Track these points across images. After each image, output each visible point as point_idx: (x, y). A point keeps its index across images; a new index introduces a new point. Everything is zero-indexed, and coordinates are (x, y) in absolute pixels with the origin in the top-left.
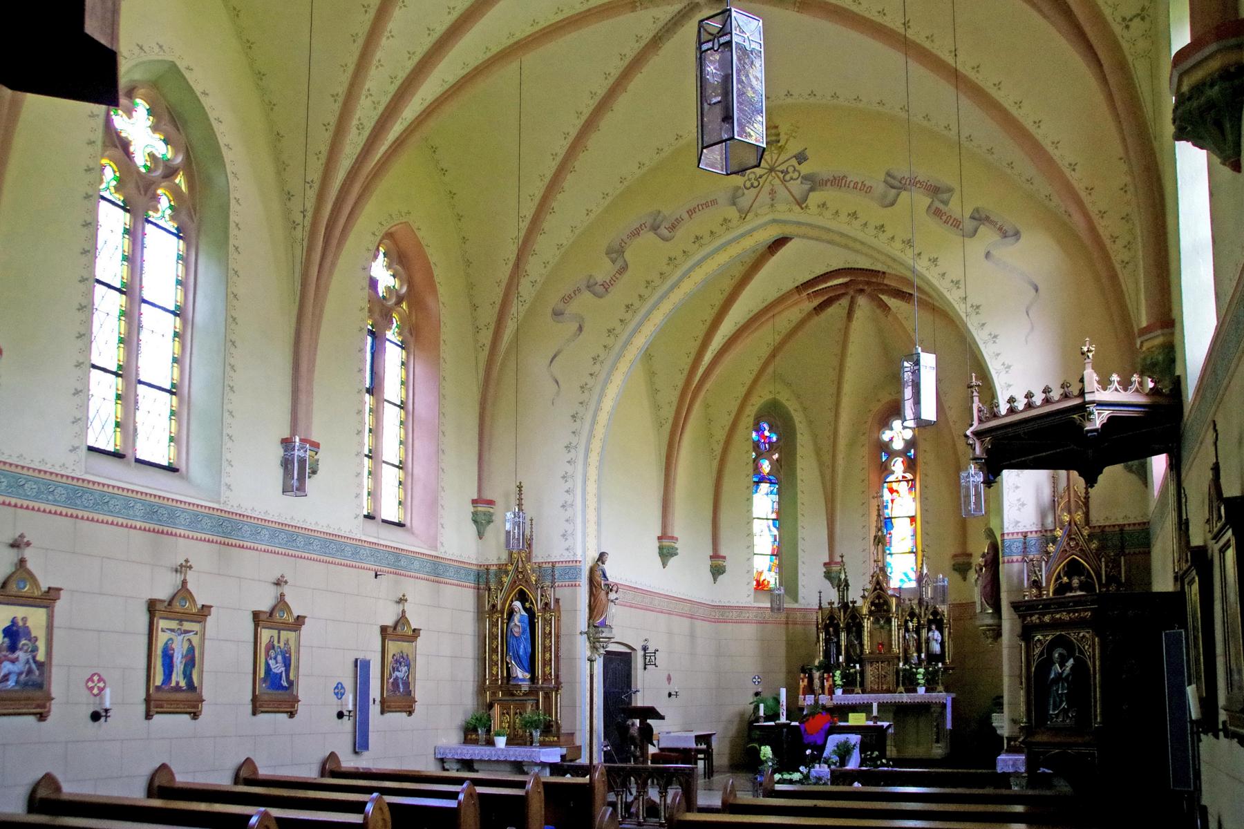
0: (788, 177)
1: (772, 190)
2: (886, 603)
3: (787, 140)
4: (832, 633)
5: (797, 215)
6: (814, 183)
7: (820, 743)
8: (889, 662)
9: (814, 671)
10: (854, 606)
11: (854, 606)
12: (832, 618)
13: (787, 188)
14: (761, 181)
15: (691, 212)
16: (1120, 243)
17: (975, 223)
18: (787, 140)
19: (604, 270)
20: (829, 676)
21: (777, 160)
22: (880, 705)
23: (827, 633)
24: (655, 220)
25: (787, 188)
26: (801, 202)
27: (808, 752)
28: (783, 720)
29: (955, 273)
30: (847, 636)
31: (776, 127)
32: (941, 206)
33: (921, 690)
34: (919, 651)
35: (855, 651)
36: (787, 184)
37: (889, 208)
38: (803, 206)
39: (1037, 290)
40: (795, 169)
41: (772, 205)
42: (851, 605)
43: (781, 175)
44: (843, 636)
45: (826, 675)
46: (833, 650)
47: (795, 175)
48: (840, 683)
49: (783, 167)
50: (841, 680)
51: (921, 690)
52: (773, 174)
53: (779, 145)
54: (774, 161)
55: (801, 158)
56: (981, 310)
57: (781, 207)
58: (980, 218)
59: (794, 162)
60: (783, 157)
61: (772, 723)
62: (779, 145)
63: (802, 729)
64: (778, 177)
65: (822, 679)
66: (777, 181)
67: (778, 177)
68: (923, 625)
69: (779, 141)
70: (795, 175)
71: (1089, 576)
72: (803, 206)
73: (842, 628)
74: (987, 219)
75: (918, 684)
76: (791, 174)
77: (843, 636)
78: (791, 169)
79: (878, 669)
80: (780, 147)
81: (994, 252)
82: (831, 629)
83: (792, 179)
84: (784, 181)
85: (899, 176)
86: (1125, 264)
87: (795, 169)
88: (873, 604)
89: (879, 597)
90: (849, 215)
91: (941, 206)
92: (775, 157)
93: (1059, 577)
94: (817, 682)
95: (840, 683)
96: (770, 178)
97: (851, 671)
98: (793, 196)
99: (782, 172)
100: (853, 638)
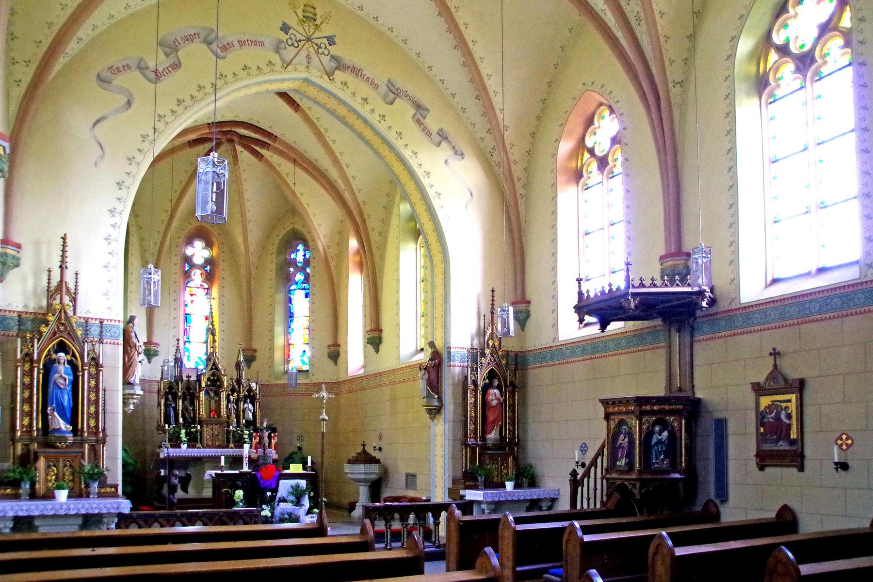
0: (320, 51)
1: (309, 55)
2: (219, 379)
3: (322, 23)
4: (171, 399)
5: (324, 82)
6: (340, 65)
7: (274, 486)
8: (221, 425)
9: (265, 431)
10: (188, 380)
11: (188, 380)
12: (171, 387)
13: (319, 58)
14: (301, 44)
15: (242, 43)
16: (522, 182)
17: (440, 138)
18: (322, 23)
19: (156, 60)
20: (275, 436)
21: (313, 34)
22: (226, 457)
23: (167, 399)
24: (209, 35)
25: (319, 58)
26: (330, 74)
27: (269, 494)
28: (246, 469)
29: (426, 167)
30: (183, 403)
31: (315, 9)
32: (421, 119)
33: (184, 446)
34: (238, 417)
35: (189, 414)
36: (322, 57)
37: (388, 105)
38: (331, 78)
39: (472, 195)
40: (326, 48)
41: (308, 67)
42: (185, 378)
43: (316, 48)
44: (180, 402)
45: (272, 435)
46: (172, 413)
47: (326, 52)
48: (186, 439)
49: (318, 41)
50: (186, 437)
51: (184, 446)
52: (309, 43)
53: (315, 23)
54: (310, 34)
55: (331, 41)
56: (441, 196)
57: (314, 71)
58: (443, 136)
59: (325, 40)
60: (318, 34)
61: (237, 472)
62: (315, 23)
63: (259, 476)
64: (313, 47)
65: (270, 437)
66: (311, 49)
67: (313, 47)
68: (242, 399)
69: (315, 20)
70: (326, 52)
71: (74, 355)
72: (331, 78)
73: (180, 396)
74: (446, 138)
75: (181, 442)
76: (323, 50)
77: (180, 402)
78: (323, 46)
79: (213, 430)
80: (316, 25)
81: (449, 161)
82: (170, 396)
83: (323, 53)
84: (317, 52)
85: (397, 86)
86: (522, 196)
87: (326, 48)
88: (209, 379)
89: (213, 375)
90: (362, 99)
91: (421, 119)
92: (312, 31)
93: (484, 379)
94: (266, 440)
95: (186, 439)
96: (307, 45)
97: (192, 430)
98: (324, 69)
99: (317, 45)
100: (188, 405)
